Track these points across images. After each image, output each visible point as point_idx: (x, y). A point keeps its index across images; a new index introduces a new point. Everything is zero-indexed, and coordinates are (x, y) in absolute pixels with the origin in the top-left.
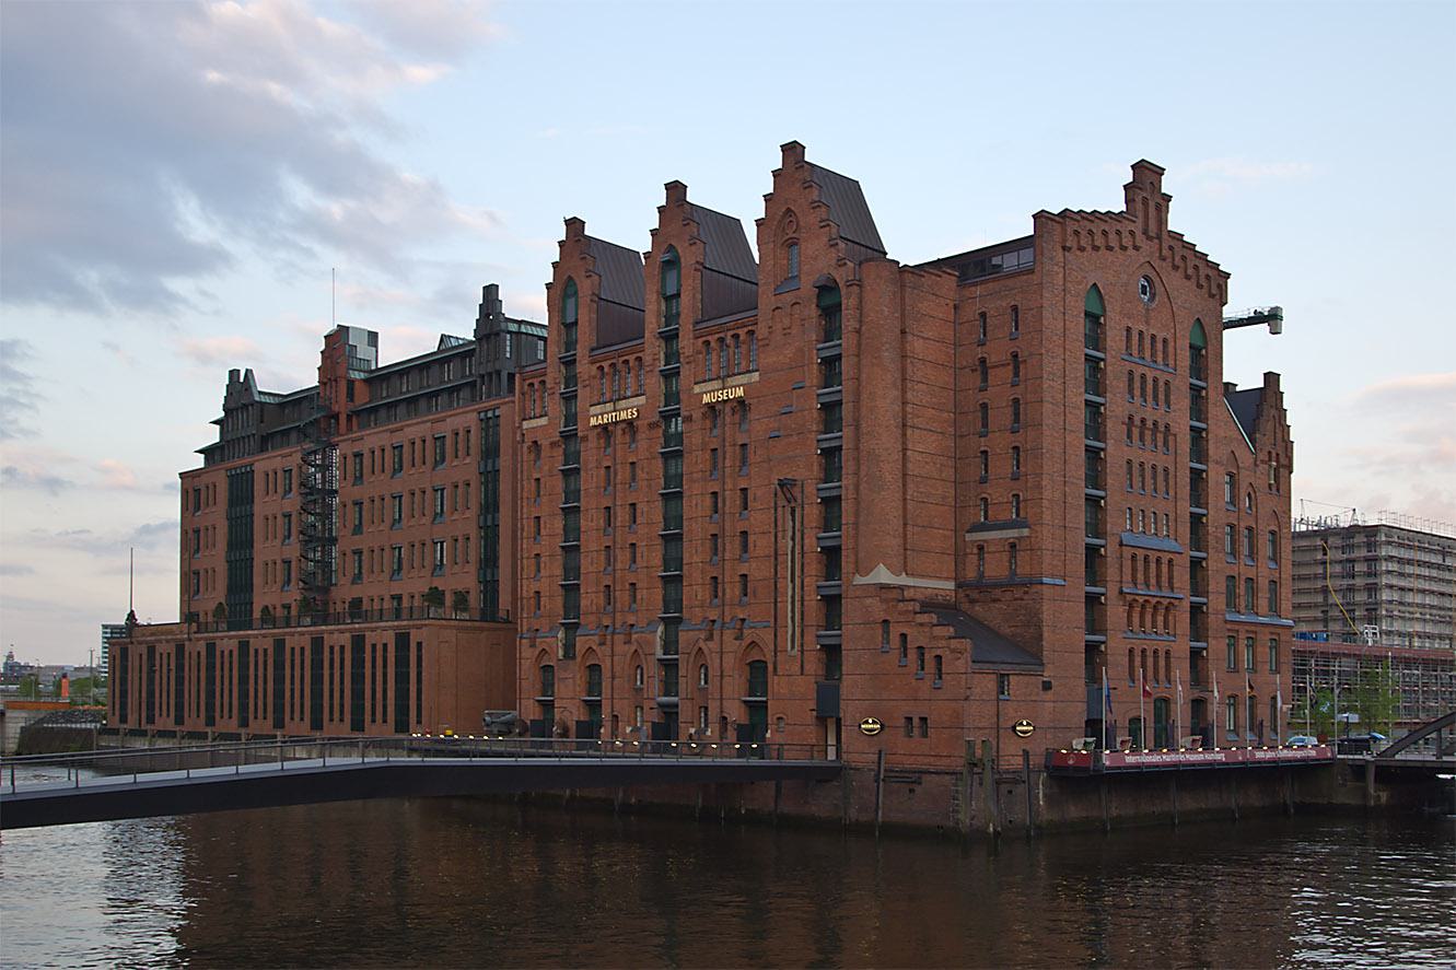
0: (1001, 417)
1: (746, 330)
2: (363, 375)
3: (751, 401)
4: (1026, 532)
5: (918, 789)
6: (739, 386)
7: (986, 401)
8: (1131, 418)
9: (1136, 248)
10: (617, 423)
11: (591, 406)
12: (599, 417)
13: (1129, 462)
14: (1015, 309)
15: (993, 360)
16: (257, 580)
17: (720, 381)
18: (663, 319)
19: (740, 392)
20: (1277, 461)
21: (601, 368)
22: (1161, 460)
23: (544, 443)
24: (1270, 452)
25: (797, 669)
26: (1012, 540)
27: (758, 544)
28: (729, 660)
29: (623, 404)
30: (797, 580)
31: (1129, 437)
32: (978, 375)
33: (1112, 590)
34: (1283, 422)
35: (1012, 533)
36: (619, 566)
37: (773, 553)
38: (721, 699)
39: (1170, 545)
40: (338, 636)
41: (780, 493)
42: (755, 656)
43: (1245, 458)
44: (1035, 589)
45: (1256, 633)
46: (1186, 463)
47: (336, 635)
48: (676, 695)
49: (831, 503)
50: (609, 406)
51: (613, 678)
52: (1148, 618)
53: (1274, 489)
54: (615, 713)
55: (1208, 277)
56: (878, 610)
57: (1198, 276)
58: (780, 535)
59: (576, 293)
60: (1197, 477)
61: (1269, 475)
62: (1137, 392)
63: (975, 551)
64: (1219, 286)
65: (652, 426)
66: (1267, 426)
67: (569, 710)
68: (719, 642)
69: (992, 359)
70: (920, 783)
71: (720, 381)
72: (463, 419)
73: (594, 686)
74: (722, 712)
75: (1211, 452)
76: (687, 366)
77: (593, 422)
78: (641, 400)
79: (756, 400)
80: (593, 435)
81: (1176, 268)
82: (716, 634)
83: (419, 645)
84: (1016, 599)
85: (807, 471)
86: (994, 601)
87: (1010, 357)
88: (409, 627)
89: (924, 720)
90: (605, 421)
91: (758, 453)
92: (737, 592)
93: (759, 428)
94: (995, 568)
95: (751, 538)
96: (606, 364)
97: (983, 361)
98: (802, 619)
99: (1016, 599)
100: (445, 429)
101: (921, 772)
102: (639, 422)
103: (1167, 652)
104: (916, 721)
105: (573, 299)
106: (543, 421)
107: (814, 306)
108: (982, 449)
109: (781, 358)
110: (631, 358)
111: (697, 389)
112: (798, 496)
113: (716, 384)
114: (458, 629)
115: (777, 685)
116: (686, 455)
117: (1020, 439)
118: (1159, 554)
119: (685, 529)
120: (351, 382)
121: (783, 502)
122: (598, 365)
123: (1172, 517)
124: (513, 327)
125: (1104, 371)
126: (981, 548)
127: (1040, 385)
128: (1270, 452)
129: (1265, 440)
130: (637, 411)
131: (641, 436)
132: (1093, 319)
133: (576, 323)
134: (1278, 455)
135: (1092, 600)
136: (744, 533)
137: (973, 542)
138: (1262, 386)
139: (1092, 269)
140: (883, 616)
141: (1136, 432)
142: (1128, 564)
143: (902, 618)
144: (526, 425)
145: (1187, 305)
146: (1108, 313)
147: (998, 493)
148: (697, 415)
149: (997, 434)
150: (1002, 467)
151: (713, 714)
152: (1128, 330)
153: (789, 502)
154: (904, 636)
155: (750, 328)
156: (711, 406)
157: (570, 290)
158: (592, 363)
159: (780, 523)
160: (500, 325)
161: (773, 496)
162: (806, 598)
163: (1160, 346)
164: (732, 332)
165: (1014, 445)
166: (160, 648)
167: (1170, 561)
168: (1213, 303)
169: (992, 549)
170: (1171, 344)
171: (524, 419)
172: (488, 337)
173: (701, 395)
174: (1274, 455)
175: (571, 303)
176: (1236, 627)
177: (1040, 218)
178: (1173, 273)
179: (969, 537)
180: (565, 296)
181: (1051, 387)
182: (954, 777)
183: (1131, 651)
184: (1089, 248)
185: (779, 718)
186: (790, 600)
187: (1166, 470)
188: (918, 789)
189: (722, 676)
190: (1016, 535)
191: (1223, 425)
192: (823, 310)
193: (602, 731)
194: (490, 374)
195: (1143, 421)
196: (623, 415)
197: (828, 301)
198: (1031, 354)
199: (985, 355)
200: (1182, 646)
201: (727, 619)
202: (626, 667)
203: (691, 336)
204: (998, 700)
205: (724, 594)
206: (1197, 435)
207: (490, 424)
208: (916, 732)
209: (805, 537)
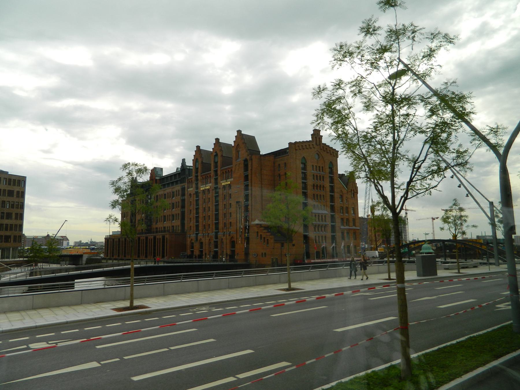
8: (314, 185)
9: (314, 148)
13: (314, 195)
14: (285, 163)
19: (229, 183)
21: (203, 178)
23: (192, 194)
28: (228, 241)
29: (207, 185)
39: (326, 212)
40: (151, 236)
42: (233, 240)
43: (345, 191)
46: (329, 194)
47: (150, 236)
49: (246, 207)
50: (204, 186)
55: (333, 152)
57: (330, 152)
59: (198, 161)
64: (336, 154)
65: (213, 190)
67: (197, 252)
72: (178, 188)
73: (201, 247)
77: (201, 189)
85: (242, 200)
88: (165, 234)
95: (232, 214)
96: (204, 177)
97: (279, 174)
100: (174, 190)
106: (192, 189)
107: (243, 164)
111: (221, 182)
113: (225, 181)
121: (238, 206)
124: (188, 168)
125: (306, 175)
131: (211, 192)
136: (231, 213)
140: (256, 231)
148: (221, 187)
151: (225, 252)
152: (313, 166)
154: (261, 235)
164: (228, 170)
166: (115, 240)
167: (325, 216)
174: (353, 190)
175: (197, 164)
177: (290, 144)
187: (324, 196)
191: (338, 184)
194: (183, 178)
201: (227, 231)
204: (281, 249)
207: (183, 189)
208: (264, 256)
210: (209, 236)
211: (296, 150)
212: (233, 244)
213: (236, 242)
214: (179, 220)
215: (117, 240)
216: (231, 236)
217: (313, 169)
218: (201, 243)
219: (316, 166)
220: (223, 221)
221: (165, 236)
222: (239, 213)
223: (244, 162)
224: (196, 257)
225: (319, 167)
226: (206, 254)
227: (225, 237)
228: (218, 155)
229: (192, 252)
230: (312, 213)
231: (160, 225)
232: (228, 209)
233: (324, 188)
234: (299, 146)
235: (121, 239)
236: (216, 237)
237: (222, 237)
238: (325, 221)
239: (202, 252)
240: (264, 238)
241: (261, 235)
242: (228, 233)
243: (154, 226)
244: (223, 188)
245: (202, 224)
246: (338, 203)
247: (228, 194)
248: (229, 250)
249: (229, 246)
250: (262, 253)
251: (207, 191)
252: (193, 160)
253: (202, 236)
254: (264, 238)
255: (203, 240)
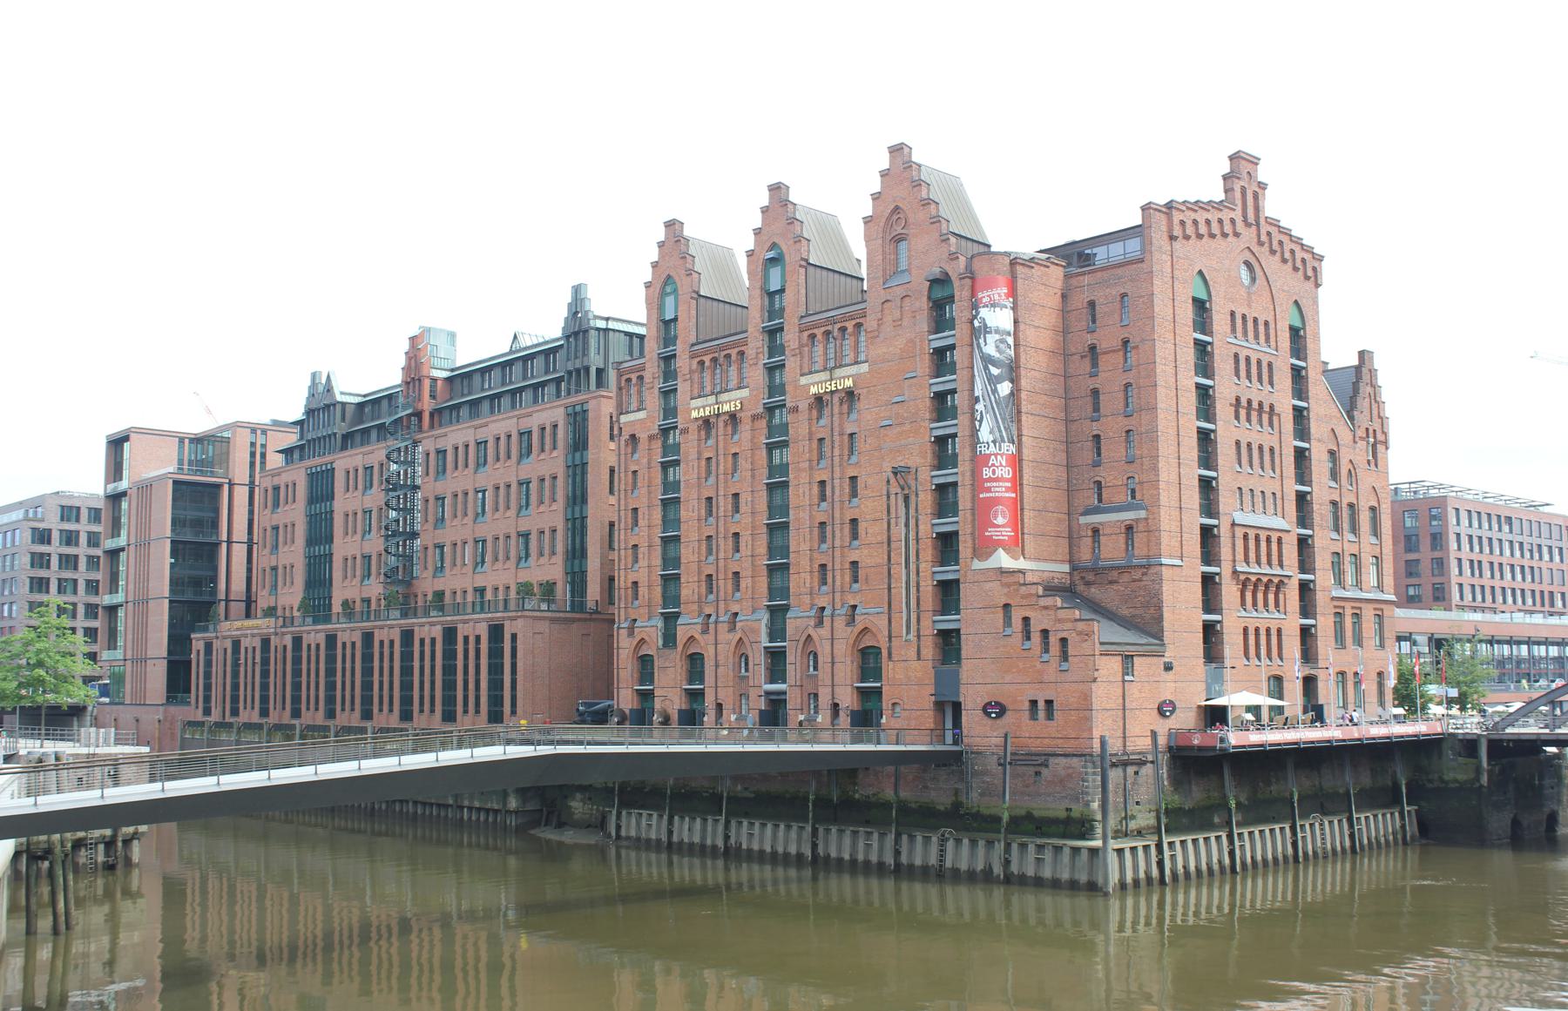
0: (1111, 401)
1: (854, 322)
2: (445, 374)
3: (860, 391)
4: (1142, 514)
5: (1045, 771)
6: (848, 377)
7: (1097, 386)
8: (1238, 399)
9: (1237, 235)
10: (718, 415)
11: (692, 399)
12: (699, 408)
15: (1103, 346)
16: (337, 575)
17: (828, 373)
18: (767, 314)
19: (849, 383)
20: (1375, 437)
21: (702, 363)
22: (1268, 440)
23: (643, 436)
24: (1367, 429)
25: (912, 653)
26: (1128, 523)
27: (870, 531)
28: (842, 648)
30: (912, 567)
31: (1237, 417)
32: (1087, 363)
33: (1225, 570)
34: (1378, 399)
35: (1129, 516)
36: (721, 555)
37: (885, 540)
38: (833, 686)
39: (1277, 522)
40: (429, 629)
41: (893, 480)
42: (867, 641)
44: (1153, 570)
45: (1360, 608)
46: (1290, 443)
47: (427, 628)
48: (784, 682)
50: (712, 399)
51: (717, 666)
52: (1260, 596)
53: (1372, 464)
54: (719, 701)
56: (1000, 596)
57: (1294, 260)
58: (893, 521)
59: (675, 291)
60: (1301, 456)
61: (1368, 453)
62: (1243, 373)
63: (1090, 533)
64: (1314, 269)
65: (755, 418)
66: (1363, 403)
68: (829, 629)
69: (1103, 345)
70: (1047, 766)
71: (828, 373)
72: (552, 413)
74: (833, 698)
75: (1313, 431)
76: (792, 359)
77: (694, 414)
78: (745, 393)
79: (865, 390)
80: (693, 427)
81: (1273, 252)
82: (827, 621)
83: (514, 637)
84: (1134, 581)
85: (919, 456)
86: (1111, 582)
87: (1120, 343)
88: (504, 619)
89: (1049, 703)
90: (707, 413)
91: (869, 441)
92: (847, 578)
93: (869, 417)
94: (1112, 549)
95: (862, 526)
96: (707, 359)
97: (1093, 348)
98: (918, 604)
99: (1134, 581)
101: (1045, 755)
102: (742, 415)
103: (1279, 631)
104: (1041, 705)
105: (672, 297)
106: (642, 415)
107: (925, 299)
108: (1095, 433)
109: (891, 349)
110: (734, 352)
111: (804, 381)
112: (912, 483)
113: (824, 376)
114: (553, 620)
115: (890, 670)
116: (791, 445)
117: (1134, 422)
118: (1269, 533)
119: (791, 517)
120: (434, 380)
121: (895, 489)
122: (699, 359)
123: (1279, 495)
124: (601, 324)
125: (1211, 354)
126: (1096, 531)
127: (1154, 370)
128: (1367, 429)
129: (1362, 418)
130: (741, 403)
132: (1201, 306)
133: (675, 319)
134: (1374, 431)
135: (1208, 581)
136: (854, 522)
137: (1087, 525)
138: (1356, 362)
139: (1194, 255)
140: (1004, 601)
141: (1243, 413)
142: (1240, 543)
143: (1024, 602)
144: (623, 419)
145: (1286, 288)
146: (1213, 298)
147: (1111, 476)
148: (803, 405)
149: (1110, 418)
150: (1113, 450)
151: (825, 700)
152: (1233, 314)
153: (903, 489)
154: (1026, 620)
155: (858, 321)
156: (819, 399)
157: (668, 289)
158: (692, 358)
159: (893, 510)
160: (589, 323)
161: (885, 483)
162: (922, 583)
163: (1261, 328)
164: (839, 325)
165: (1127, 428)
167: (1280, 540)
168: (1310, 285)
169: (1107, 531)
170: (1272, 326)
171: (621, 414)
172: (576, 334)
173: (808, 386)
174: (1371, 431)
175: (670, 301)
176: (1342, 604)
178: (1271, 258)
179: (1083, 520)
180: (663, 294)
181: (1163, 372)
182: (1083, 759)
183: (1245, 630)
184: (1193, 236)
185: (894, 704)
186: (904, 585)
187: (1272, 450)
188: (1045, 771)
189: (833, 663)
190: (1133, 517)
191: (1323, 406)
192: (934, 302)
193: (705, 719)
195: (1249, 402)
196: (726, 408)
197: (939, 293)
198: (1143, 340)
199: (1095, 342)
200: (1292, 622)
201: (838, 605)
202: (731, 655)
203: (797, 329)
204: (1124, 681)
205: (834, 582)
206: (1300, 415)
207: (578, 420)
208: (1041, 714)
209: (920, 523)
210: (739, 625)
211: (1172, 238)
212: (869, 661)
213: (885, 653)
214: (559, 559)
215: (257, 643)
216: (860, 627)
217: (1234, 330)
218: (695, 664)
219: (1244, 317)
220: (811, 560)
221: (502, 626)
222: (903, 520)
223: (930, 288)
224: (666, 721)
225: (1255, 320)
226: (719, 707)
227: (824, 632)
228: (787, 258)
229: (646, 696)
230: (1233, 524)
231: (457, 581)
232: (842, 502)
233: (1275, 419)
234: (1182, 223)
235: (274, 641)
236: (777, 632)
237: (811, 631)
238: (1281, 565)
239: (696, 696)
240: (1045, 633)
241: (1026, 620)
242: (843, 611)
243: (426, 584)
244: (810, 407)
245: (699, 573)
246: (1322, 490)
247: (841, 434)
248: (849, 689)
249: (847, 671)
250: (1034, 703)
251: (726, 425)
252: (648, 285)
253: (699, 628)
254: (1045, 633)
255: (705, 645)
